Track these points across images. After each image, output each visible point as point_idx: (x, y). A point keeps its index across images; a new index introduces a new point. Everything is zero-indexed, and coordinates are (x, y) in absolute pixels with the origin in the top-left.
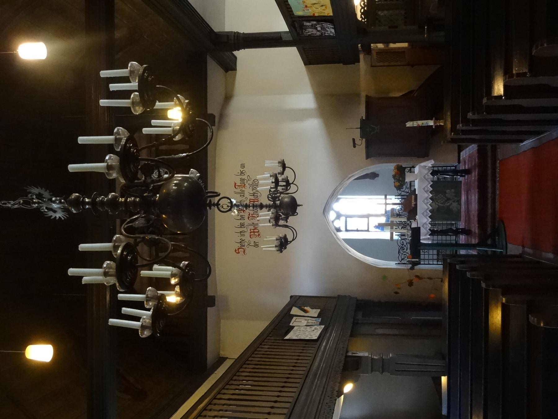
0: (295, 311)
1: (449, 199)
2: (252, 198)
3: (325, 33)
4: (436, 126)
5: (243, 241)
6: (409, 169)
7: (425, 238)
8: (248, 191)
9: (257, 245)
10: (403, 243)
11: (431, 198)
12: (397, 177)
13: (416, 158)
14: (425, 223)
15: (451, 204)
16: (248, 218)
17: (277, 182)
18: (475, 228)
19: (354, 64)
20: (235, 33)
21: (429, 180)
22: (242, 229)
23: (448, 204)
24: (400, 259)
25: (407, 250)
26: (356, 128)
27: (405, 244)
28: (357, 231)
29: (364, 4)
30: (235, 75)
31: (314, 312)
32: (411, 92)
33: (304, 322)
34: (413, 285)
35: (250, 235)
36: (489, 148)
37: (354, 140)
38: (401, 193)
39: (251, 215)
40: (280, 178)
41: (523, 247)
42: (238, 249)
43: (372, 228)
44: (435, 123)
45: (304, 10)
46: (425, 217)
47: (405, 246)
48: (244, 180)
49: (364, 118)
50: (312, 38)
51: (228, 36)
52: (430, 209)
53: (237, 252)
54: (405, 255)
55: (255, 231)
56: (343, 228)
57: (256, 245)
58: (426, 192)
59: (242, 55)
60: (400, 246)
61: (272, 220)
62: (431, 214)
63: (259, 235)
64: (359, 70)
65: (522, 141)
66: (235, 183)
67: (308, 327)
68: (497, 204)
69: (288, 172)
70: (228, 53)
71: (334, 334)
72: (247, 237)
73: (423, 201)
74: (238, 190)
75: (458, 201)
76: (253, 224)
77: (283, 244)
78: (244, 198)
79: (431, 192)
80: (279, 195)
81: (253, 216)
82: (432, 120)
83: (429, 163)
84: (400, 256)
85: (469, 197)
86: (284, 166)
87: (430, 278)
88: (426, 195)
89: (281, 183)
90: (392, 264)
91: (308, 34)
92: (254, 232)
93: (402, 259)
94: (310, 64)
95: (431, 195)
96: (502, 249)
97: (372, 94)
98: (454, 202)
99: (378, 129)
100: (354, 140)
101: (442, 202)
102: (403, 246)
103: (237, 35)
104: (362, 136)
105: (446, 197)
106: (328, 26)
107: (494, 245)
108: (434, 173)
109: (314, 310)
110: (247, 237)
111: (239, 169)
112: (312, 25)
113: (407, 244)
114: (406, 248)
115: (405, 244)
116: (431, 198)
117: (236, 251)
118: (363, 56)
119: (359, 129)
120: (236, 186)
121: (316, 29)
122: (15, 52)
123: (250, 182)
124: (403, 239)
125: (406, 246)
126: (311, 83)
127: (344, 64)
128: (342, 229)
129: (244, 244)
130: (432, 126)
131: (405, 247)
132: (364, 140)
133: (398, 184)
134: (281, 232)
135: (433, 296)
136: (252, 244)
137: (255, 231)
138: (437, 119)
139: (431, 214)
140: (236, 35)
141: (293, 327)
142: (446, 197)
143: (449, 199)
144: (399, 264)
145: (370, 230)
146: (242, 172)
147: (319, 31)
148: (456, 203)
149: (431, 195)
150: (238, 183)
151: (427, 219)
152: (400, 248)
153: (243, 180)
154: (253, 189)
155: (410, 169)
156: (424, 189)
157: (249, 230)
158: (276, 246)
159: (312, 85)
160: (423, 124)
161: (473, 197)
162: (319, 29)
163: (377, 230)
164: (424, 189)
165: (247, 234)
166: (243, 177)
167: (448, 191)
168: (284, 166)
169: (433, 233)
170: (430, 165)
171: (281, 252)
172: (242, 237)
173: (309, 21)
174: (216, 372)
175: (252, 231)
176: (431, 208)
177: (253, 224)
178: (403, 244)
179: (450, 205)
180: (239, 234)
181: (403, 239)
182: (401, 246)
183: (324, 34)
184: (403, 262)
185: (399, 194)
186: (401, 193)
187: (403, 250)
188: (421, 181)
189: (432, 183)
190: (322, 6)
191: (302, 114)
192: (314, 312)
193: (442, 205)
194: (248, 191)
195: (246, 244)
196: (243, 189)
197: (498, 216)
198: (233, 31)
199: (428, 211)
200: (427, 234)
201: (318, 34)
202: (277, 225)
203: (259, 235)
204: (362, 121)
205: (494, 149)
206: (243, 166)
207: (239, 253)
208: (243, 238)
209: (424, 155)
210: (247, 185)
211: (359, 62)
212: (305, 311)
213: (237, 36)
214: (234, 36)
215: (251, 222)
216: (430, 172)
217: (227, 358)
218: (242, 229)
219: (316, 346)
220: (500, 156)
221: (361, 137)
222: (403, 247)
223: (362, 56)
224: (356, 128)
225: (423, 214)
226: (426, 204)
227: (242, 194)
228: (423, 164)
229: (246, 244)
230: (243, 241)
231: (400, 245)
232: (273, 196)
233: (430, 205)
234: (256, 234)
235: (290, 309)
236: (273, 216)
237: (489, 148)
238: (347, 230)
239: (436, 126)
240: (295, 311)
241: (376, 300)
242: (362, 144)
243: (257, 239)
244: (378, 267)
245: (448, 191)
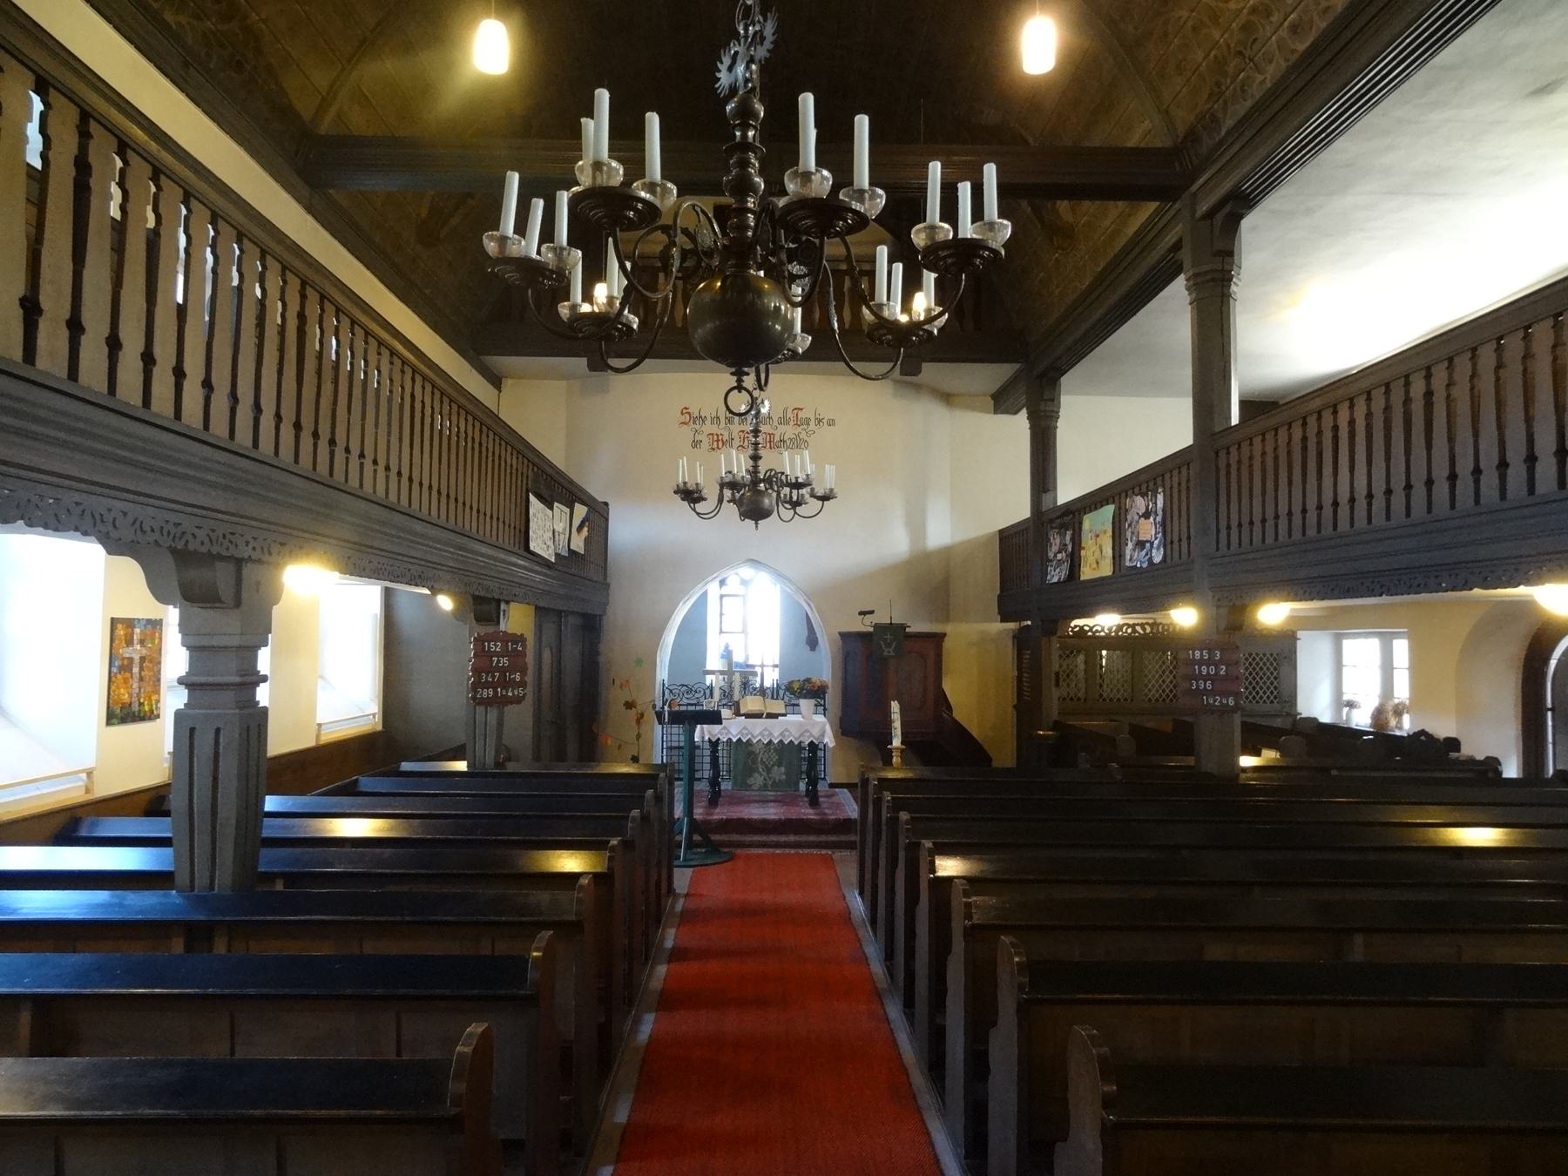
0: (581, 511)
1: (769, 770)
2: (777, 438)
3: (1052, 566)
4: (891, 751)
5: (703, 421)
6: (822, 703)
7: (703, 733)
8: (789, 431)
9: (696, 446)
11: (770, 741)
12: (808, 686)
13: (840, 714)
14: (729, 732)
15: (761, 775)
16: (743, 431)
17: (798, 486)
18: (721, 813)
19: (999, 613)
20: (1058, 412)
21: (802, 739)
22: (723, 420)
23: (761, 770)
24: (671, 688)
27: (697, 695)
28: (721, 614)
29: (1097, 631)
30: (983, 410)
31: (578, 544)
32: (949, 707)
33: (560, 526)
34: (627, 709)
35: (713, 434)
36: (853, 838)
37: (872, 612)
39: (746, 435)
40: (804, 491)
41: (687, 895)
42: (689, 413)
43: (725, 638)
44: (897, 749)
45: (1090, 532)
46: (740, 732)
48: (808, 424)
49: (907, 630)
50: (1043, 543)
51: (1053, 400)
52: (752, 739)
53: (684, 411)
55: (720, 443)
56: (725, 590)
57: (696, 444)
58: (782, 734)
59: (1018, 426)
61: (730, 476)
62: (744, 741)
63: (713, 449)
64: (988, 620)
65: (861, 893)
66: (802, 409)
67: (551, 534)
68: (760, 851)
69: (815, 505)
70: (1023, 399)
71: (538, 578)
72: (709, 428)
73: (765, 729)
74: (789, 415)
75: (765, 785)
76: (733, 439)
77: (690, 495)
78: (776, 423)
79: (781, 741)
80: (776, 489)
81: (746, 440)
82: (902, 743)
83: (829, 740)
85: (772, 804)
86: (824, 498)
87: (639, 736)
88: (776, 735)
89: (795, 492)
90: (662, 674)
91: (1052, 538)
92: (718, 441)
93: (671, 691)
94: (1001, 540)
95: (776, 742)
96: (685, 860)
97: (948, 644)
98: (765, 780)
99: (889, 652)
100: (872, 612)
101: (765, 760)
103: (1054, 416)
104: (876, 626)
105: (773, 766)
106: (1064, 573)
107: (691, 845)
108: (813, 746)
109: (582, 545)
110: (709, 428)
111: (826, 416)
112: (1066, 545)
115: (697, 695)
116: (770, 741)
117: (686, 408)
119: (889, 622)
120: (796, 411)
121: (1060, 552)
122: (1038, 13)
123: (803, 435)
124: (705, 693)
126: (969, 541)
128: (724, 588)
129: (697, 422)
130: (891, 744)
132: (871, 629)
133: (796, 686)
134: (711, 492)
135: (609, 742)
136: (698, 438)
137: (720, 443)
138: (902, 751)
139: (744, 741)
140: (1055, 414)
141: (552, 509)
142: (773, 766)
143: (769, 770)
144: (664, 685)
145: (722, 635)
146: (820, 421)
147: (1055, 556)
148: (761, 783)
149: (776, 742)
150: (802, 415)
151: (737, 735)
153: (807, 422)
154: (791, 440)
155: (821, 705)
156: (787, 730)
157: (722, 432)
158: (685, 483)
159: (963, 543)
160: (895, 729)
161: (772, 811)
162: (1059, 556)
163: (723, 648)
164: (787, 730)
165: (714, 429)
166: (812, 423)
167: (783, 769)
168: (824, 498)
169: (714, 745)
170: (826, 740)
171: (676, 492)
172: (709, 418)
173: (1072, 539)
174: (474, 371)
175: (720, 437)
176: (755, 741)
177: (733, 439)
178: (696, 692)
179: (759, 772)
180: (714, 415)
181: (705, 693)
183: (1050, 564)
184: (667, 692)
188: (800, 724)
189: (796, 743)
190: (1097, 563)
191: (917, 526)
192: (578, 544)
193: (759, 759)
194: (789, 431)
195: (698, 427)
196: (792, 423)
197: (739, 851)
198: (1061, 410)
199: (749, 736)
200: (712, 735)
201: (1051, 555)
202: (722, 485)
203: (713, 449)
204: (903, 627)
205: (850, 846)
206: (831, 423)
207: (682, 414)
208: (708, 422)
209: (845, 729)
210: (799, 429)
211: (1002, 621)
212: (580, 529)
213: (1053, 416)
214: (1053, 411)
215: (735, 434)
216: (815, 741)
217: (500, 392)
218: (723, 420)
219: (516, 549)
220: (838, 855)
221: (876, 624)
223: (1012, 626)
225: (745, 728)
226: (761, 734)
227: (784, 421)
228: (828, 728)
229: (698, 427)
230: (703, 421)
231: (696, 687)
232: (774, 479)
233: (760, 740)
234: (715, 443)
235: (583, 503)
236: (738, 478)
237: (853, 838)
238: (722, 597)
239: (891, 751)
240: (581, 511)
241: (602, 648)
242: (864, 626)
243: (705, 445)
244: (658, 652)
245: (783, 769)
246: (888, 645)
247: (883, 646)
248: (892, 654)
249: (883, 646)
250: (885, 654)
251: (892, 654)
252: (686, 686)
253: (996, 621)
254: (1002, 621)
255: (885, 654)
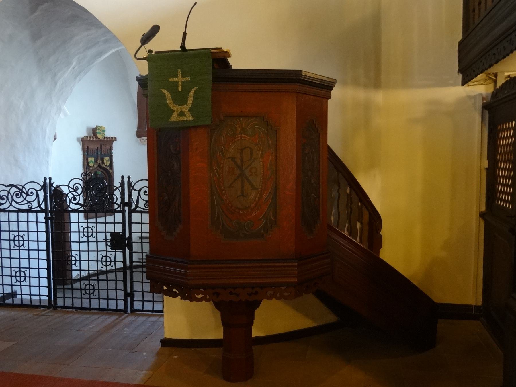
10: (29, 193)
25: (17, 203)
26: (185, 34)
27: (28, 198)
38: (135, 190)
47: (25, 199)
54: (7, 198)
60: (23, 187)
84: (5, 188)
99: (182, 114)
102: (24, 195)
113: (29, 202)
114: (18, 200)
118: (481, 94)
124: (38, 196)
125: (25, 202)
127: (460, 43)
131: (21, 199)
152: (21, 187)
178: (27, 194)
182: (24, 190)
185: (133, 184)
186: (135, 190)
187: (17, 195)
222: (21, 195)
224: (185, 34)
231: (27, 187)
246: (180, 99)
247: (170, 102)
248: (189, 117)
249: (170, 102)
250: (174, 117)
251: (189, 117)
252: (15, 186)
253: (454, 85)
254: (464, 82)
255: (174, 117)
